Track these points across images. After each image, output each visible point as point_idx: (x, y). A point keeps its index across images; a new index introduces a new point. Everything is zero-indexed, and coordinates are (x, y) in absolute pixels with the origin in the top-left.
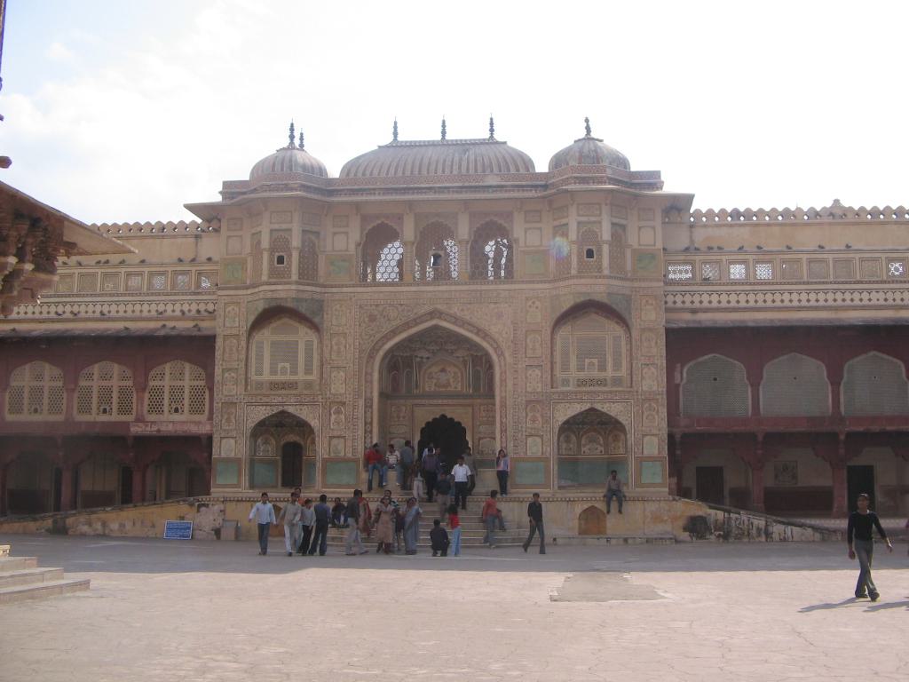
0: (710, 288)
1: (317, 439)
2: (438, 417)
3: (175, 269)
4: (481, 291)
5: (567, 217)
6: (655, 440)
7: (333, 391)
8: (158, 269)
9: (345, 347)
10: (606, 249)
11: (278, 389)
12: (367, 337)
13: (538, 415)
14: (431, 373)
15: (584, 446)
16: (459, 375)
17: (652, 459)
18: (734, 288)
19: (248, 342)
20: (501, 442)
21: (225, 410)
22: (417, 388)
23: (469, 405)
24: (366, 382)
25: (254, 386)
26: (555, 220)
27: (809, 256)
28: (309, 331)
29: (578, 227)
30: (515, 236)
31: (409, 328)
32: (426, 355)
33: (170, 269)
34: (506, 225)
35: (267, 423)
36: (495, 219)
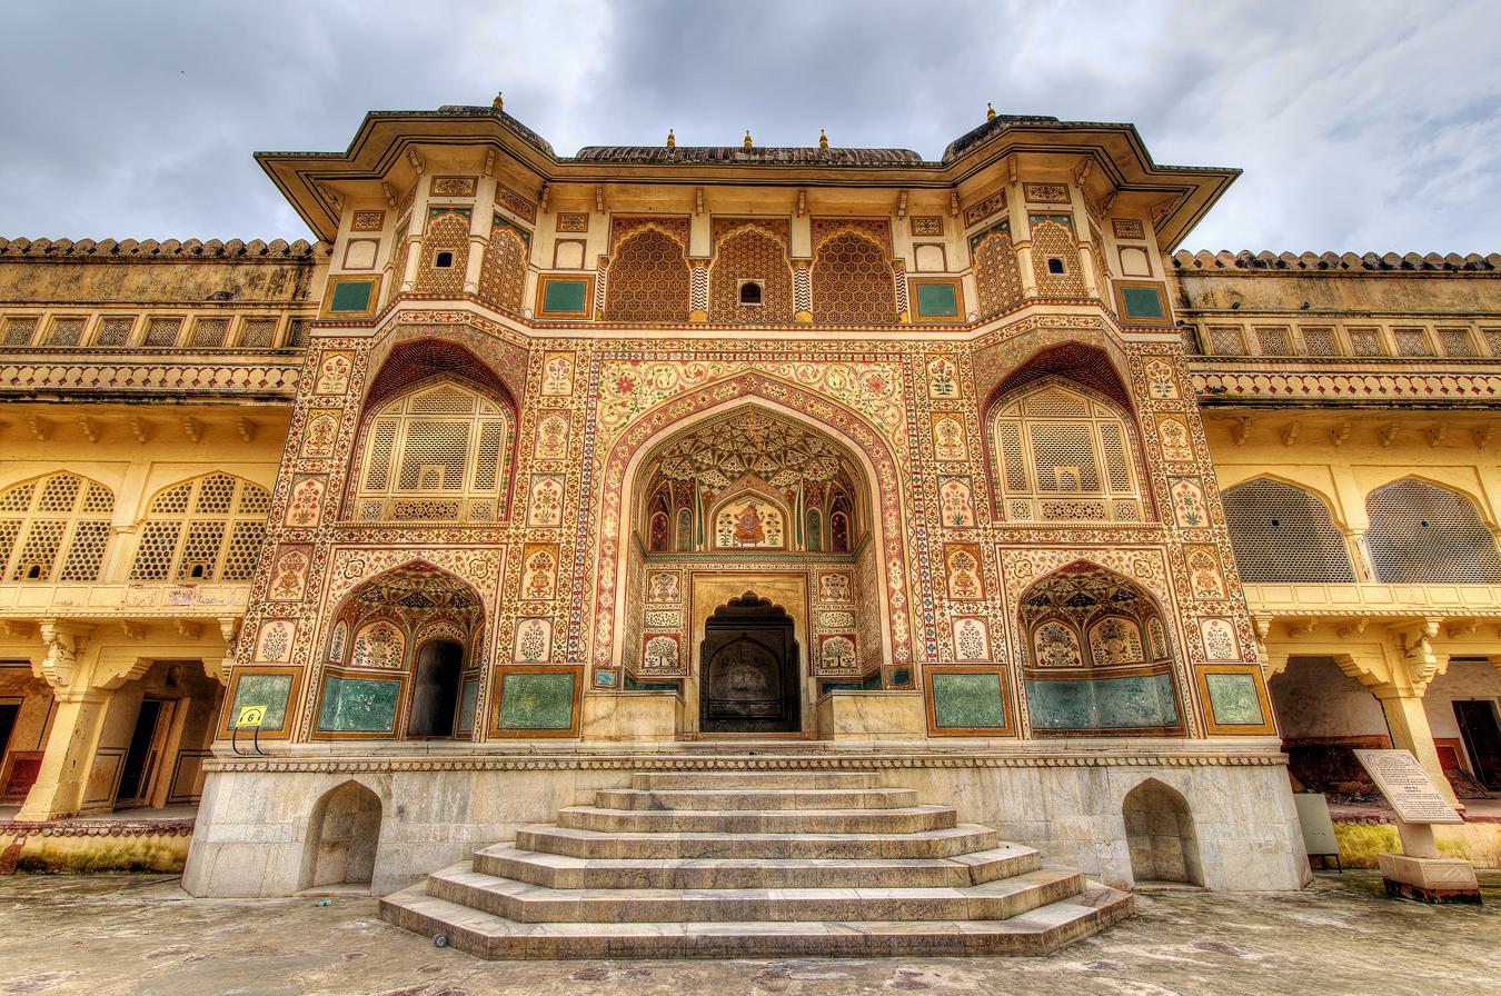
0: (1234, 367)
1: (488, 626)
2: (740, 597)
3: (248, 312)
5: (1005, 206)
6: (1225, 626)
7: (533, 521)
8: (217, 312)
9: (567, 436)
10: (1086, 257)
11: (413, 516)
12: (614, 418)
13: (972, 573)
15: (1041, 650)
16: (779, 518)
17: (1227, 668)
18: (1276, 367)
19: (361, 422)
20: (893, 633)
21: (282, 561)
22: (701, 542)
23: (799, 575)
25: (360, 512)
27: (1392, 322)
28: (489, 403)
29: (1031, 225)
31: (699, 409)
32: (718, 480)
33: (239, 313)
35: (384, 592)
36: (858, 232)
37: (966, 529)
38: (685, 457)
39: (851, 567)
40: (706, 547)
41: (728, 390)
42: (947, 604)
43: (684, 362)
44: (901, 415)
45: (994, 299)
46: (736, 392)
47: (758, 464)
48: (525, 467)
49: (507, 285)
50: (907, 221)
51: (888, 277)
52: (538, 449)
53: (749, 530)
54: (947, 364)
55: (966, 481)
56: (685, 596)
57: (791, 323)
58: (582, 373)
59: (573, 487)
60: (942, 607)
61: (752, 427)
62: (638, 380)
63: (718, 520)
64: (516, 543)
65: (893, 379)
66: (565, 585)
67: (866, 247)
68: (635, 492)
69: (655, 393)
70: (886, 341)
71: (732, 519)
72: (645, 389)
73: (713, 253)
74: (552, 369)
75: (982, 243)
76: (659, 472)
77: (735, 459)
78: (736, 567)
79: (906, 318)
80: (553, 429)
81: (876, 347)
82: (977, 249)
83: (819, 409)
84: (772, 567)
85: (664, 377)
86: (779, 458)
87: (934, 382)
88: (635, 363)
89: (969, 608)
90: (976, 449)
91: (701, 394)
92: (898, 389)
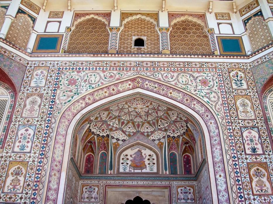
2: (132, 199)
4: (184, 62)
7: (17, 149)
9: (40, 106)
12: (65, 98)
14: (127, 155)
16: (155, 157)
22: (111, 169)
23: (165, 187)
24: (56, 142)
26: (242, 15)
30: (211, 26)
31: (111, 95)
32: (122, 136)
34: (199, 22)
36: (190, 18)
37: (259, 155)
38: (104, 122)
39: (195, 183)
40: (114, 172)
41: (126, 85)
42: (252, 197)
43: (104, 72)
44: (219, 97)
45: (259, 44)
46: (131, 87)
47: (143, 128)
48: (16, 121)
49: (21, 38)
50: (213, 15)
51: (206, 37)
52: (24, 112)
53: (138, 163)
54: (240, 73)
55: (256, 129)
56: (102, 198)
57: (159, 53)
58: (51, 76)
59: (39, 132)
60: (249, 199)
61: (140, 107)
62: (79, 80)
63: (121, 158)
64: (5, 161)
65: (213, 80)
66: (29, 185)
67: (195, 25)
68: (75, 139)
69: (88, 86)
70: (208, 63)
71: (129, 157)
72: (83, 84)
73: (121, 25)
74: (37, 75)
75: (250, 21)
76: (89, 130)
77: (130, 125)
78: (130, 183)
79: (217, 52)
80: (33, 102)
81: (203, 65)
82: (247, 24)
83: (175, 94)
84: (150, 183)
85: (93, 78)
86: (154, 124)
87: (234, 81)
88: (78, 72)
89: (265, 200)
90: (259, 113)
91: (112, 87)
92: (216, 84)
